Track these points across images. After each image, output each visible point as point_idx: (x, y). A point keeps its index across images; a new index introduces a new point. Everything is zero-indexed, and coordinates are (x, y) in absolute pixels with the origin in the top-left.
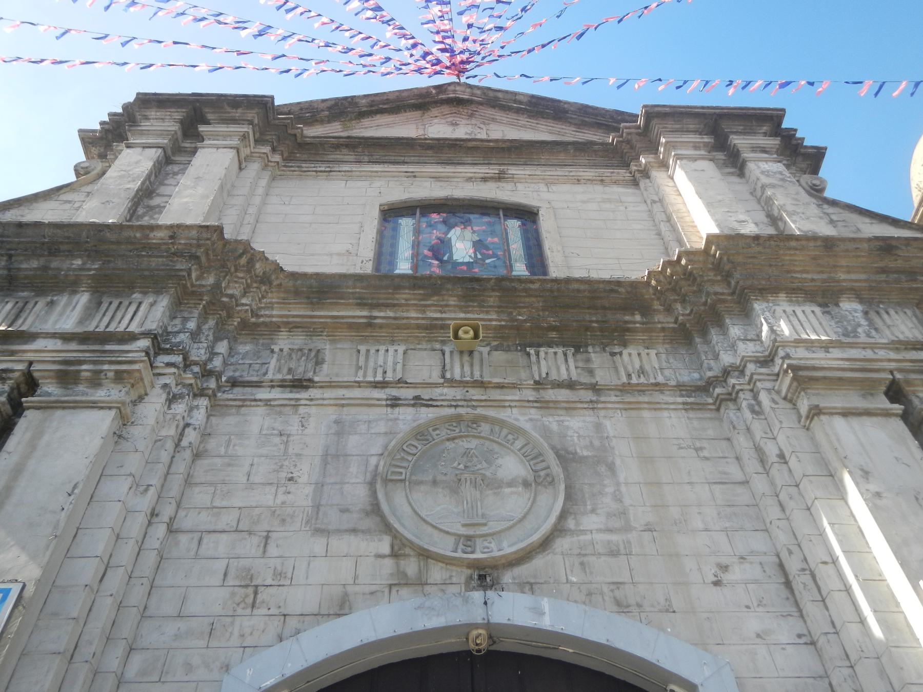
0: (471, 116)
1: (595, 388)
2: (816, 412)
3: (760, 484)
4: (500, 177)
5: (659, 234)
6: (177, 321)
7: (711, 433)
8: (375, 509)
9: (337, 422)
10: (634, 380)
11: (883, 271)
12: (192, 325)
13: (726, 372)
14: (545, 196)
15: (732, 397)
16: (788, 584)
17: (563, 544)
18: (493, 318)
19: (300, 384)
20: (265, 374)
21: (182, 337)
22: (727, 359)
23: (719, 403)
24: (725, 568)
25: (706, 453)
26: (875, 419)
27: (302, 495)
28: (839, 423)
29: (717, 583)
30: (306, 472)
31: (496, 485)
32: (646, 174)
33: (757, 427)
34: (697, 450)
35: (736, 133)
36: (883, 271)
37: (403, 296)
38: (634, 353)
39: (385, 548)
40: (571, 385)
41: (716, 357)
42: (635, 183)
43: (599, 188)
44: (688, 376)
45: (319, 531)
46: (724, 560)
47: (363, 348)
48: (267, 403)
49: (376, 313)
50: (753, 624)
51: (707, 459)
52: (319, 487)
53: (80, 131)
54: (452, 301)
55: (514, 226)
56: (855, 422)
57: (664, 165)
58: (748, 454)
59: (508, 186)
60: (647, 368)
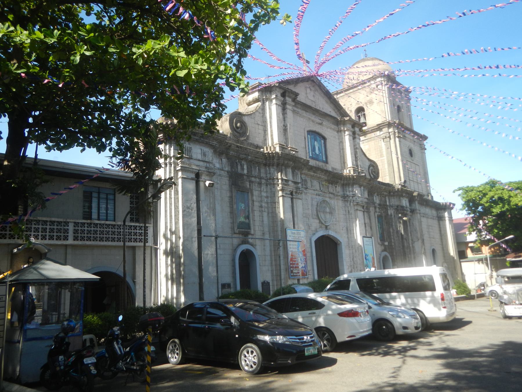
0: (313, 86)
1: (334, 194)
2: (357, 210)
3: (348, 216)
4: (321, 124)
5: (340, 151)
8: (318, 215)
9: (311, 198)
11: (368, 183)
13: (347, 196)
15: (347, 201)
16: (347, 230)
18: (326, 178)
22: (348, 193)
23: (345, 201)
27: (310, 212)
28: (358, 212)
30: (310, 207)
31: (326, 213)
32: (341, 131)
33: (349, 208)
36: (368, 183)
37: (319, 172)
40: (332, 193)
41: (346, 191)
42: (338, 132)
45: (313, 218)
49: (315, 174)
52: (312, 210)
54: (323, 174)
57: (345, 131)
58: (347, 211)
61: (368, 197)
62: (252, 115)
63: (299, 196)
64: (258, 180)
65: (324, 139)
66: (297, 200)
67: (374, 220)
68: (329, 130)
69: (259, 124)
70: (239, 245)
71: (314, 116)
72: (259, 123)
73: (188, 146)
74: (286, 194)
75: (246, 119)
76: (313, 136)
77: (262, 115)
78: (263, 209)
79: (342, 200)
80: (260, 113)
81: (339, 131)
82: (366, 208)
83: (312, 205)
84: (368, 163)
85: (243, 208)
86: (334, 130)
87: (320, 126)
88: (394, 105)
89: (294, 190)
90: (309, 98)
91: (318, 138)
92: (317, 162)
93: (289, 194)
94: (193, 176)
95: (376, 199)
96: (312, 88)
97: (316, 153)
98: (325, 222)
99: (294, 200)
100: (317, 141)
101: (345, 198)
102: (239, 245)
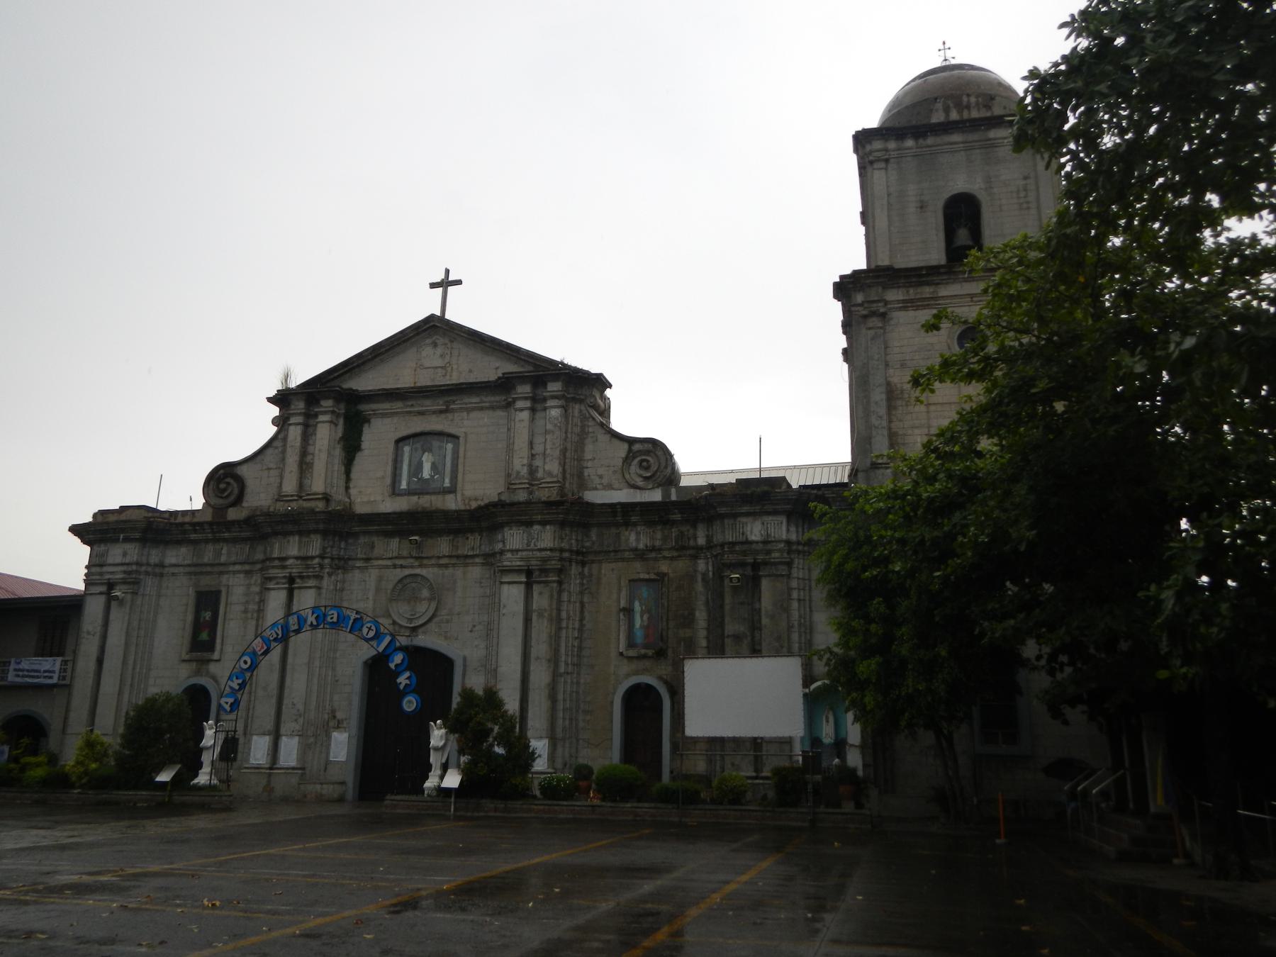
2: (502, 583)
4: (446, 411)
6: (326, 542)
7: (487, 576)
10: (469, 554)
12: (331, 543)
14: (466, 422)
17: (436, 620)
19: (368, 560)
20: (357, 554)
21: (329, 550)
24: (474, 626)
25: (482, 585)
26: (517, 585)
27: (370, 604)
28: (505, 587)
29: (471, 631)
30: (371, 595)
34: (481, 583)
35: (549, 381)
38: (473, 538)
39: (391, 622)
43: (490, 413)
44: (486, 549)
46: (475, 624)
47: (386, 540)
48: (359, 568)
50: (476, 643)
51: (482, 587)
53: (270, 399)
55: (450, 446)
56: (511, 586)
59: (450, 416)
60: (475, 547)
61: (550, 545)
62: (259, 458)
63: (311, 583)
64: (247, 567)
65: (457, 437)
66: (303, 590)
67: (615, 596)
68: (474, 414)
69: (269, 469)
70: (189, 677)
71: (428, 402)
72: (272, 465)
73: (104, 548)
74: (277, 583)
75: (243, 471)
76: (418, 445)
77: (280, 450)
78: (249, 615)
79: (483, 564)
80: (276, 448)
81: (508, 405)
82: (531, 577)
83: (378, 590)
84: (623, 449)
85: (207, 618)
86: (492, 408)
87: (443, 416)
88: (922, 207)
89: (293, 575)
90: (427, 365)
91: (436, 443)
92: (415, 498)
93: (284, 584)
94: (103, 589)
95: (638, 540)
96: (441, 341)
97: (421, 480)
98: (410, 620)
99: (296, 592)
100: (430, 450)
101: (490, 559)
102: (189, 677)
